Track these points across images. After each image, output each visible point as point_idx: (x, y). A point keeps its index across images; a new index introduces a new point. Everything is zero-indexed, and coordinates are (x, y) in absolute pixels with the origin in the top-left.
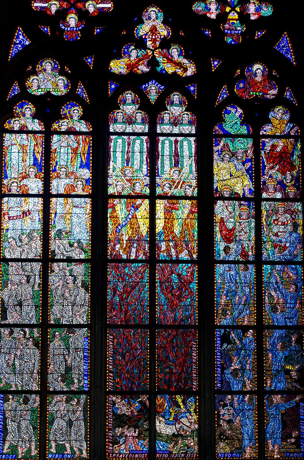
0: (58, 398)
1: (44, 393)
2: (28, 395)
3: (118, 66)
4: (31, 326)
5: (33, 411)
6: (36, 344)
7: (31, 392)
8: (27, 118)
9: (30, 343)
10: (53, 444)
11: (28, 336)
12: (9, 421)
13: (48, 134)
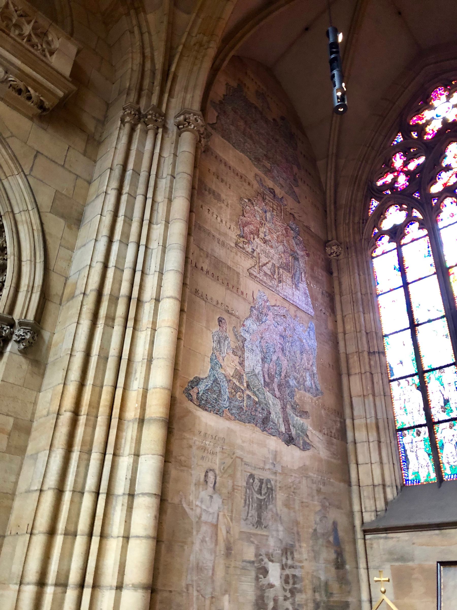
0: (442, 426)
1: (431, 424)
2: (419, 429)
3: (436, 188)
4: (413, 375)
5: (425, 440)
6: (418, 388)
7: (420, 426)
8: (385, 244)
9: (414, 387)
10: (447, 466)
11: (411, 384)
12: (408, 453)
13: (399, 248)
